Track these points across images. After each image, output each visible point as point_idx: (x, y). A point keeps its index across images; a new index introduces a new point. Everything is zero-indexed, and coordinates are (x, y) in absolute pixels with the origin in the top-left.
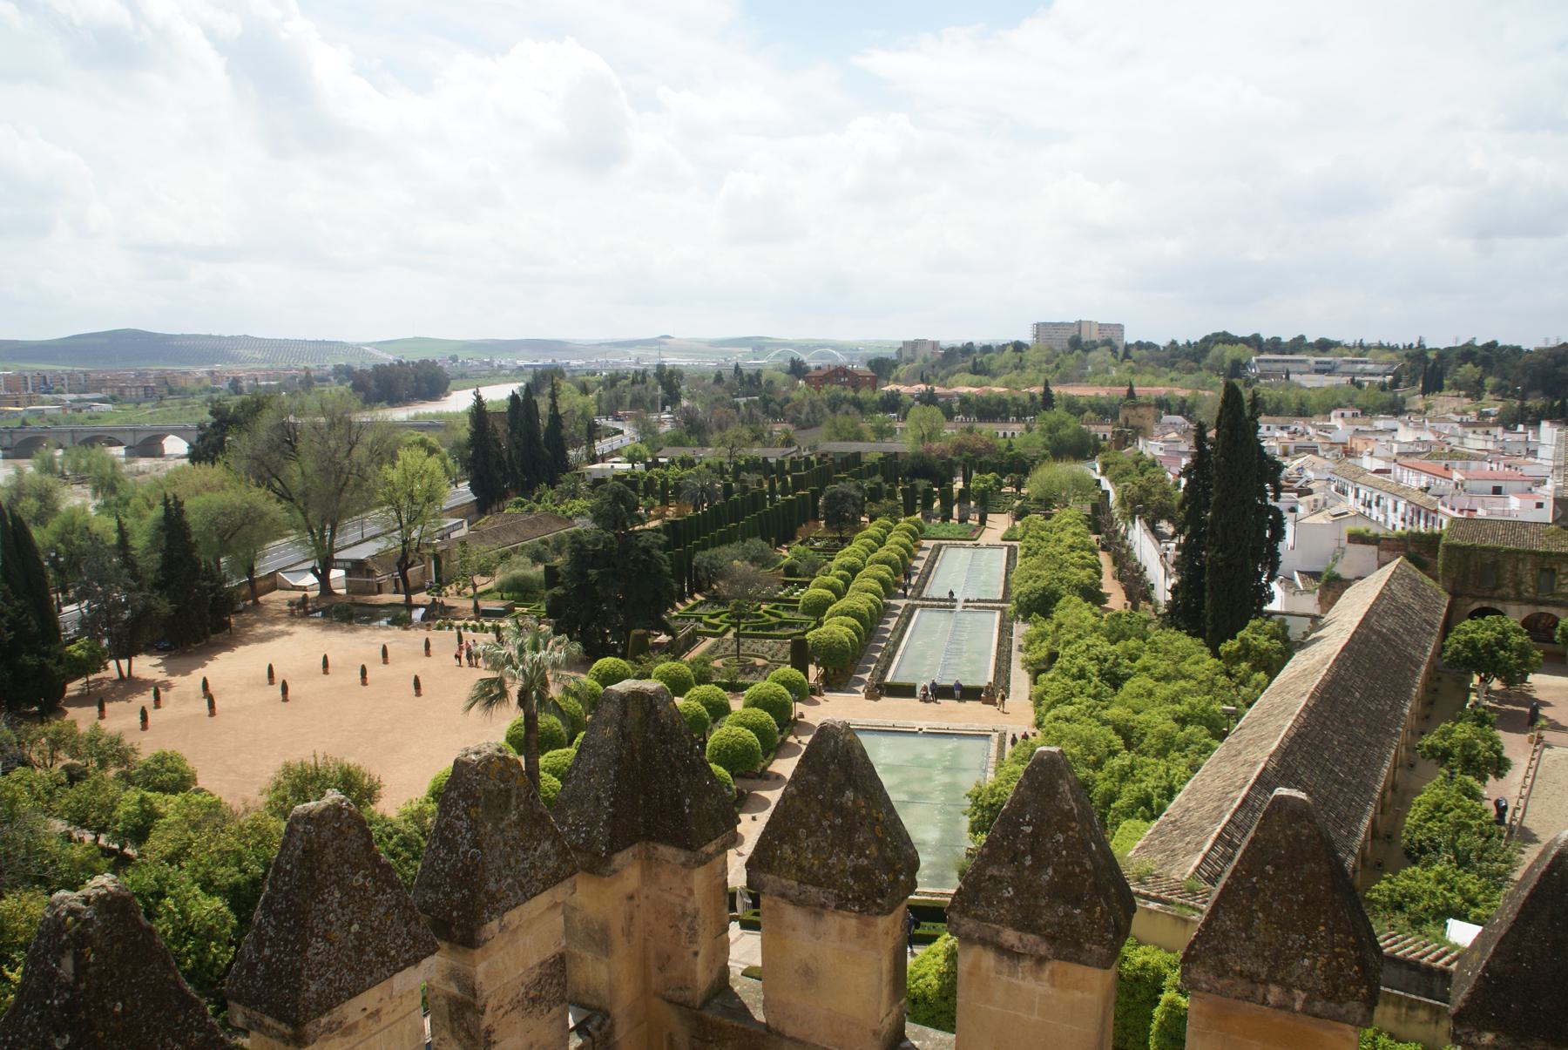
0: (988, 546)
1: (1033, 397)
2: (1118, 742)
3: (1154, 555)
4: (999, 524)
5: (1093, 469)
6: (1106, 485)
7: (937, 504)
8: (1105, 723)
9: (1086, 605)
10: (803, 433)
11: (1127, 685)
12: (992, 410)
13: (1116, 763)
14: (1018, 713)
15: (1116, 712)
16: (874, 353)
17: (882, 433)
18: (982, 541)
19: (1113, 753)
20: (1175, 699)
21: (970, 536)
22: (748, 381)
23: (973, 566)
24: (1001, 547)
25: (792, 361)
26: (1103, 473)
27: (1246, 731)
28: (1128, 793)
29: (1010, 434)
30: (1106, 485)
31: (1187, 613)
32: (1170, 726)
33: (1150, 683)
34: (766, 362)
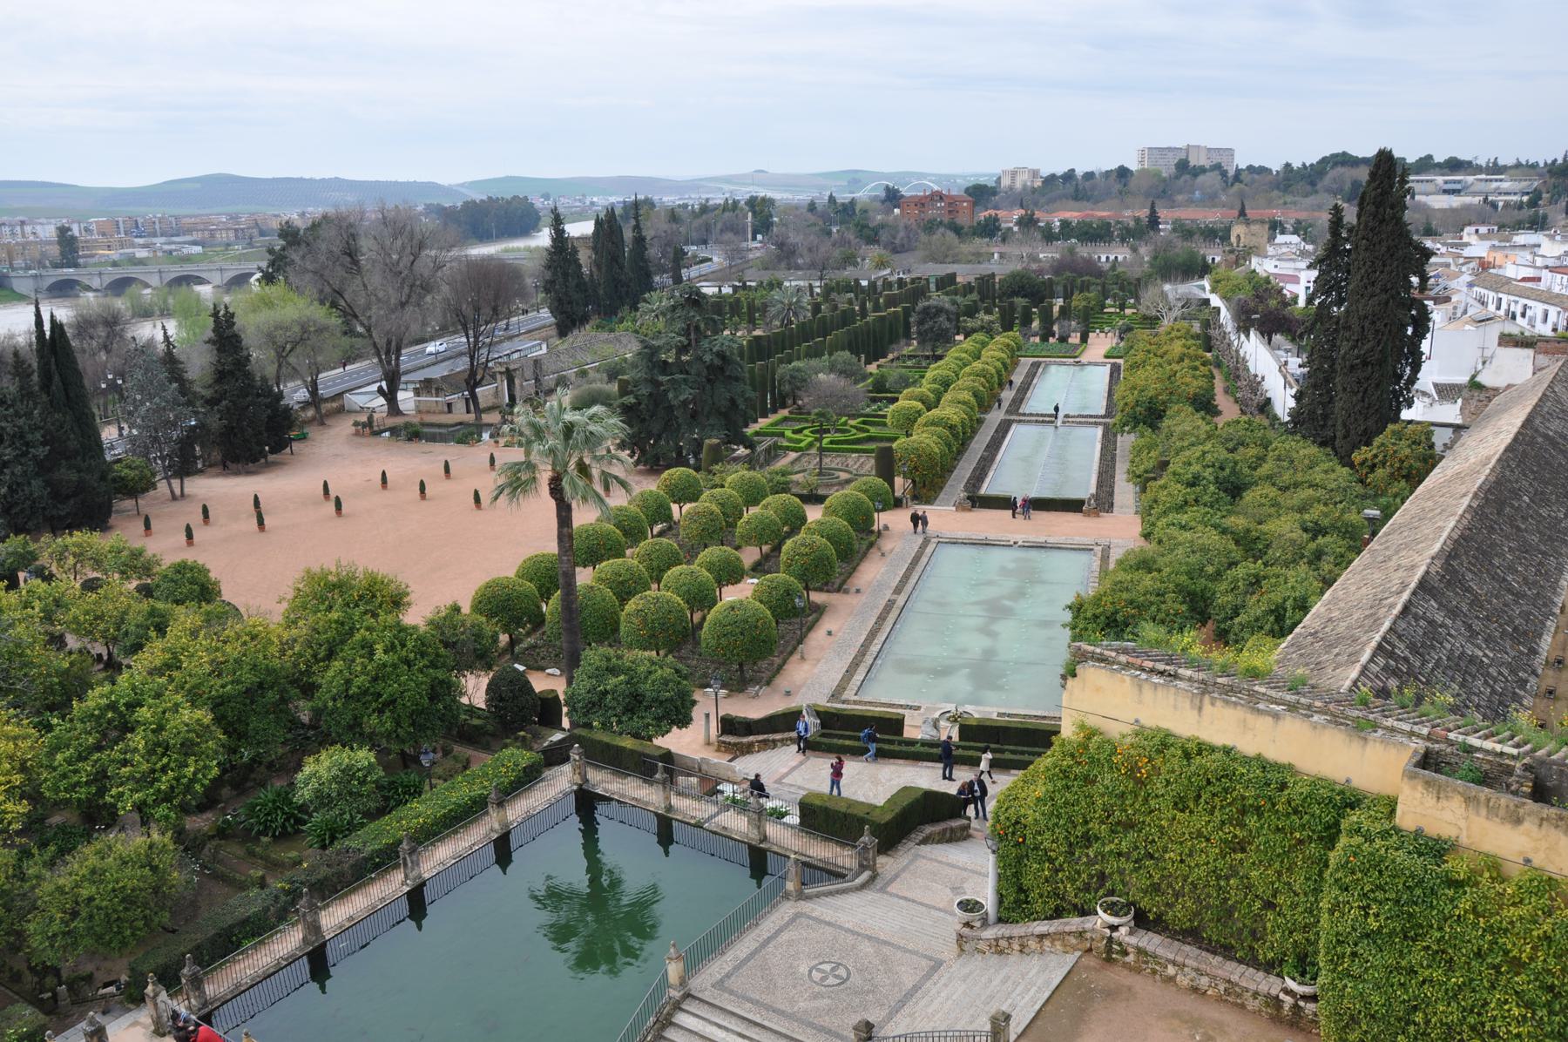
0: (1090, 364)
1: (1137, 220)
2: (1237, 554)
3: (1274, 369)
4: (1101, 344)
5: (1202, 288)
6: (1216, 301)
7: (1035, 324)
8: (1224, 532)
9: (1198, 415)
10: (896, 257)
11: (1248, 496)
12: (1097, 234)
13: (1240, 571)
14: (1122, 530)
15: (1238, 522)
16: (972, 181)
17: (978, 257)
18: (1084, 359)
19: (1232, 564)
20: (1302, 509)
21: (1071, 355)
22: (846, 211)
23: (1077, 383)
24: (1104, 364)
25: (887, 189)
26: (1213, 291)
27: (1395, 536)
28: (1256, 607)
29: (1110, 255)
30: (1216, 301)
31: (1312, 417)
32: (1299, 535)
33: (1273, 492)
34: (862, 195)
